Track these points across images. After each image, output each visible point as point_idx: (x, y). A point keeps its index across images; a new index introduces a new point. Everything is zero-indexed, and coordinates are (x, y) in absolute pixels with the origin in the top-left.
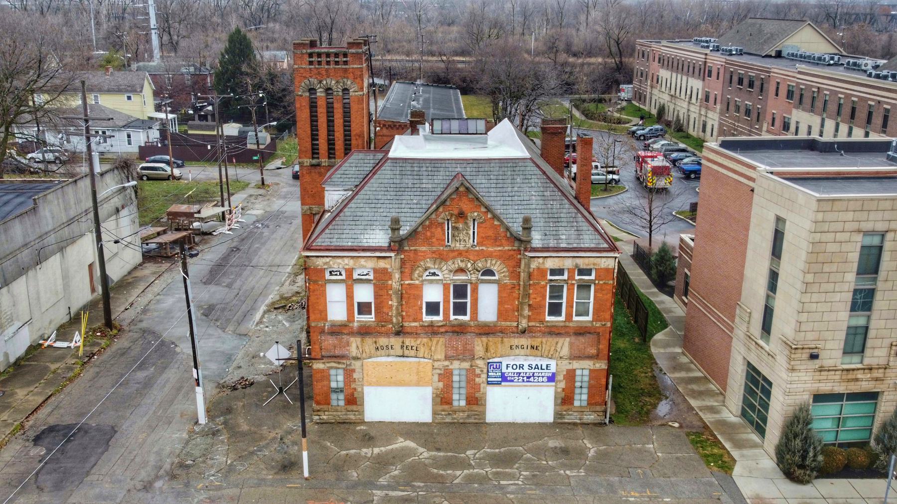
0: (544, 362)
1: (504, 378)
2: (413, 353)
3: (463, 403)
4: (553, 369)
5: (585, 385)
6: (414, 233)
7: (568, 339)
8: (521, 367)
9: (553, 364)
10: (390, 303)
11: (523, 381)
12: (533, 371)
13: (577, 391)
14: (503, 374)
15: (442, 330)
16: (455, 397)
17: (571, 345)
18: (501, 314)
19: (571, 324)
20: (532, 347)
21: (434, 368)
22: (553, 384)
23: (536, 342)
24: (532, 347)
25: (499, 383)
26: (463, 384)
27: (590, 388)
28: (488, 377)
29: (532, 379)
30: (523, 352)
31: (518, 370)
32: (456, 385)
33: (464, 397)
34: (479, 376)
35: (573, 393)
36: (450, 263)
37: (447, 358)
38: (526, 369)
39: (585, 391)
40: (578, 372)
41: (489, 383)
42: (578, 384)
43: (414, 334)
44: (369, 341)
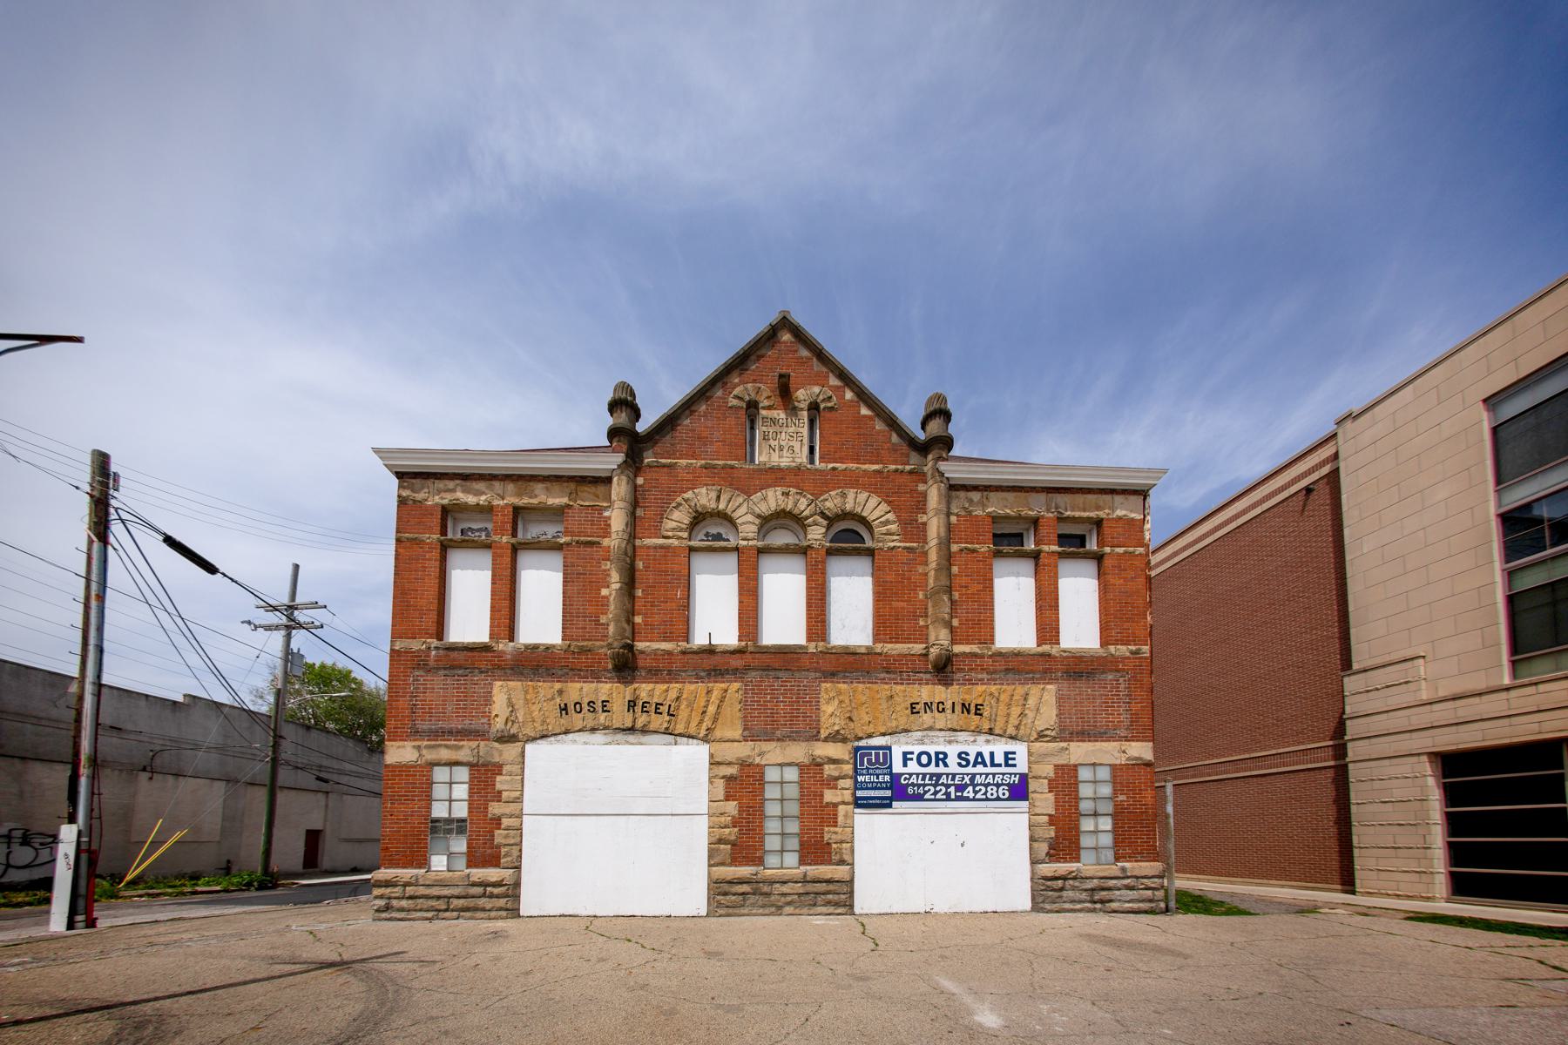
0: (999, 748)
1: (899, 791)
3: (792, 859)
4: (1022, 766)
5: (1108, 807)
8: (941, 758)
9: (1021, 750)
11: (948, 794)
12: (970, 770)
13: (1087, 825)
14: (896, 778)
15: (736, 662)
16: (772, 843)
17: (1060, 700)
18: (884, 625)
19: (1054, 651)
21: (714, 763)
22: (1025, 804)
23: (976, 693)
24: (965, 708)
25: (885, 804)
26: (793, 808)
27: (1117, 816)
28: (857, 786)
29: (969, 792)
30: (941, 720)
31: (932, 769)
32: (772, 809)
33: (794, 843)
34: (832, 782)
36: (757, 497)
37: (750, 735)
38: (953, 765)
39: (1106, 824)
40: (1084, 774)
41: (859, 803)
42: (1085, 806)
43: (665, 670)
44: (546, 688)
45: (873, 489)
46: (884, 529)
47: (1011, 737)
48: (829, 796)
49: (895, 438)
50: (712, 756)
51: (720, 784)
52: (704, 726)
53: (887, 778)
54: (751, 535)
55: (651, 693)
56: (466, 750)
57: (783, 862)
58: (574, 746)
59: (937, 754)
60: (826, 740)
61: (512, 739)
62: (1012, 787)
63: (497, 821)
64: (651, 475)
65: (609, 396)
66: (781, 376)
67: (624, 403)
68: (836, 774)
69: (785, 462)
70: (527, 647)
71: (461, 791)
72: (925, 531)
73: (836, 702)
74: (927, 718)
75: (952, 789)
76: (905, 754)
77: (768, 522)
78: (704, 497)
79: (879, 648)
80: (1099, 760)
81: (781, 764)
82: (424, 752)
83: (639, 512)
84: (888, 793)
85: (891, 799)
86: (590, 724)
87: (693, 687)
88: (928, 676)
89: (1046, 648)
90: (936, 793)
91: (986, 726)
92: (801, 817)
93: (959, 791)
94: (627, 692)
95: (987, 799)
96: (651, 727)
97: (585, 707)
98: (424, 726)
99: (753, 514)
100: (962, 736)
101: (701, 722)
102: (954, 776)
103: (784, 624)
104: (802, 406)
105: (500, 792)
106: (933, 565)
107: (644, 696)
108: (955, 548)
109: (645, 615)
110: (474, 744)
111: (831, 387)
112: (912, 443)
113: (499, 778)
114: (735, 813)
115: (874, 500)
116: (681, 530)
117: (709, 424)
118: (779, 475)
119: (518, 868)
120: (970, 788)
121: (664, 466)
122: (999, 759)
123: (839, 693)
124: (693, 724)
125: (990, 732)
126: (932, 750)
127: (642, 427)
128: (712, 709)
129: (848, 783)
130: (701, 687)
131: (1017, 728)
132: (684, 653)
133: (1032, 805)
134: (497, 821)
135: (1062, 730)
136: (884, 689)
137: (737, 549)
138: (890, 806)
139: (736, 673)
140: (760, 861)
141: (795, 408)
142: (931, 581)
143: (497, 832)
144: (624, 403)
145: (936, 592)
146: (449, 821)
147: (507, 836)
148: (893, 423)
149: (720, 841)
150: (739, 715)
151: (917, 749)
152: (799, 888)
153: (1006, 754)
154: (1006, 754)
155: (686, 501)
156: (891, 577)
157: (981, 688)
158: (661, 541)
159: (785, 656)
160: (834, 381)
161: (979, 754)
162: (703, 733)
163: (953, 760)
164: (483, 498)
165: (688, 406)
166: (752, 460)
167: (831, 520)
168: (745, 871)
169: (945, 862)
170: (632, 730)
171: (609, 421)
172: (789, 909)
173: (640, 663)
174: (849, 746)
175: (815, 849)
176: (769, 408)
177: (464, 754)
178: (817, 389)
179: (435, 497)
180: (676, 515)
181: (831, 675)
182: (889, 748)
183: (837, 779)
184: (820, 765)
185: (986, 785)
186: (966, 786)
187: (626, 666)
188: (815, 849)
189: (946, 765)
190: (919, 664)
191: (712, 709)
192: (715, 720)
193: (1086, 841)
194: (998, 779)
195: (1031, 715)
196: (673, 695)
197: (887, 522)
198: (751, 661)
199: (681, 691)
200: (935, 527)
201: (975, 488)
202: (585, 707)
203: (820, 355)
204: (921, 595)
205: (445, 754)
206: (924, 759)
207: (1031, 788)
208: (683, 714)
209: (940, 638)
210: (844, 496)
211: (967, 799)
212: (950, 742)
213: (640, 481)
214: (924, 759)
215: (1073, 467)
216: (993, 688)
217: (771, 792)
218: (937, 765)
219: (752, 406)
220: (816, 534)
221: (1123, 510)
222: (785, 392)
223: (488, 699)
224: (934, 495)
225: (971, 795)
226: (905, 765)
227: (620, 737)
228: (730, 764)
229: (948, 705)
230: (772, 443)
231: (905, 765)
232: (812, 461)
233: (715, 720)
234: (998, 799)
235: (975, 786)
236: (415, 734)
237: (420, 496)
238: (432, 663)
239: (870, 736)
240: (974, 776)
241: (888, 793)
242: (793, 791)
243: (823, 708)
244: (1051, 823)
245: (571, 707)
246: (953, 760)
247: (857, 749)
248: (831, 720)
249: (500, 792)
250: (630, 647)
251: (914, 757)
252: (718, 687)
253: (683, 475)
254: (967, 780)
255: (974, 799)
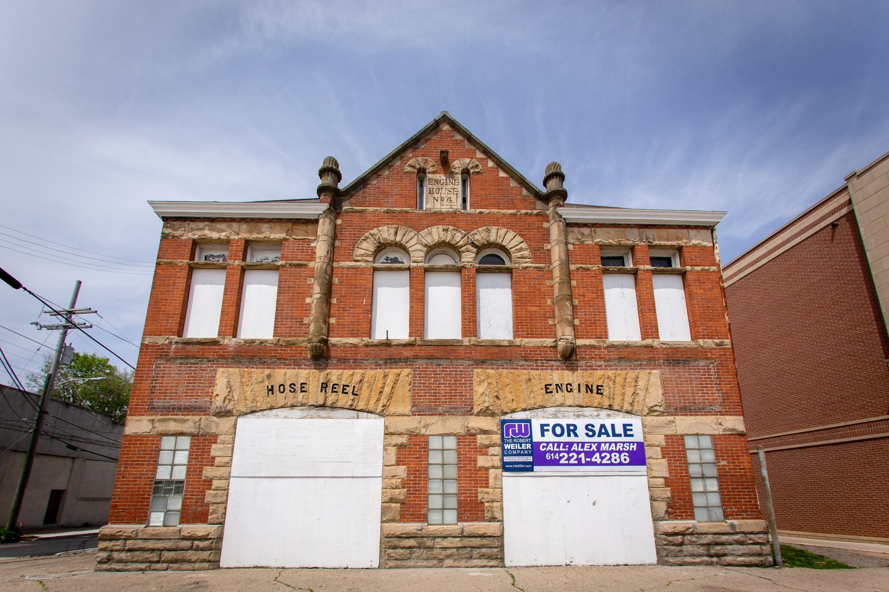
0: (619, 421)
1: (540, 457)
2: (345, 400)
3: (451, 516)
4: (638, 437)
6: (362, 183)
7: (656, 372)
8: (572, 429)
9: (636, 423)
10: (308, 300)
11: (579, 460)
12: (596, 439)
15: (407, 353)
16: (435, 502)
17: (664, 382)
20: (589, 388)
21: (388, 434)
22: (644, 468)
23: (596, 377)
25: (527, 468)
26: (452, 472)
29: (596, 458)
30: (570, 398)
31: (565, 438)
32: (435, 472)
33: (453, 502)
35: (689, 488)
37: (418, 411)
40: (690, 442)
42: (694, 470)
43: (351, 359)
44: (258, 373)
45: (510, 226)
46: (519, 254)
47: (628, 412)
48: (482, 461)
49: (524, 192)
50: (386, 428)
51: (393, 451)
52: (381, 404)
53: (529, 446)
54: (420, 259)
55: (340, 377)
56: (190, 424)
57: (443, 519)
58: (276, 420)
59: (568, 426)
60: (478, 414)
61: (227, 413)
62: (631, 453)
63: (209, 483)
64: (346, 217)
65: (320, 166)
66: (442, 152)
67: (331, 170)
68: (487, 442)
69: (445, 208)
70: (246, 341)
71: (182, 457)
72: (550, 255)
73: (486, 384)
74: (558, 397)
75: (582, 456)
76: (542, 426)
77: (432, 250)
78: (386, 233)
79: (518, 341)
80: (702, 431)
81: (442, 434)
82: (157, 424)
83: (337, 243)
84: (530, 459)
85: (533, 464)
86: (290, 401)
87: (373, 372)
88: (558, 363)
89: (649, 341)
90: (569, 459)
91: (606, 403)
92: (458, 479)
93: (588, 457)
94: (321, 376)
95: (612, 464)
96: (339, 404)
97: (288, 388)
98: (158, 403)
99: (421, 244)
100: (588, 411)
101: (378, 400)
102: (583, 444)
103: (444, 321)
104: (457, 171)
105: (213, 458)
106: (558, 280)
107: (334, 379)
108: (573, 267)
109: (338, 318)
110: (197, 418)
111: (477, 159)
112: (538, 195)
113: (214, 446)
114: (404, 475)
115: (511, 234)
116: (368, 255)
117: (391, 183)
118: (441, 217)
119: (222, 524)
120: (597, 455)
121: (357, 212)
122: (619, 430)
123: (488, 377)
124: (372, 402)
125: (610, 408)
126: (564, 422)
127: (342, 186)
128: (387, 390)
129: (497, 450)
130: (379, 372)
131: (632, 404)
132: (366, 346)
133: (650, 469)
134: (209, 483)
135: (668, 406)
136: (524, 374)
137: (409, 269)
138: (531, 470)
139: (407, 361)
140: (424, 518)
141: (452, 172)
142: (556, 292)
143: (208, 492)
144: (331, 170)
145: (560, 300)
146: (170, 482)
147: (215, 496)
148: (522, 182)
149: (392, 500)
150: (409, 394)
151: (552, 422)
152: (457, 542)
153: (625, 426)
154: (625, 426)
155: (372, 235)
156: (526, 289)
157: (600, 373)
158: (353, 264)
159: (445, 348)
160: (479, 155)
161: (603, 426)
162: (380, 408)
163: (581, 431)
164: (224, 234)
165: (376, 172)
166: (421, 207)
167: (479, 248)
168: (411, 527)
169: (580, 515)
170: (323, 406)
171: (319, 182)
172: (448, 562)
173: (333, 354)
174: (497, 419)
175: (471, 508)
176: (434, 173)
177: (188, 427)
178: (467, 160)
179: (189, 234)
180: (365, 245)
181: (481, 363)
182: (529, 421)
183: (487, 447)
184: (473, 435)
185: (611, 452)
186: (593, 453)
187: (321, 356)
188: (471, 508)
189: (576, 435)
190: (550, 354)
191: (387, 390)
192: (390, 398)
193: (698, 501)
194: (620, 447)
195: (642, 394)
196: (357, 378)
197: (521, 249)
198: (419, 352)
199: (363, 376)
200: (557, 253)
201: (585, 225)
202: (288, 388)
203: (470, 138)
204: (549, 302)
205: (173, 426)
206: (558, 430)
207: (647, 455)
208: (364, 394)
209: (565, 334)
210: (488, 231)
211: (595, 464)
212: (578, 416)
213: (339, 222)
214: (558, 430)
215: (656, 211)
216: (610, 373)
217: (434, 458)
218: (569, 435)
219: (422, 172)
220: (469, 258)
221: (697, 239)
222: (445, 162)
223: (212, 382)
224: (555, 230)
225: (598, 461)
226: (543, 435)
227: (313, 412)
228: (400, 434)
229: (575, 386)
230: (436, 196)
231: (543, 435)
232: (465, 208)
233: (390, 398)
234: (621, 464)
235: (601, 453)
236: (152, 409)
237: (177, 233)
238: (171, 354)
239: (513, 411)
240: (599, 444)
241: (530, 459)
242: (452, 457)
243: (476, 388)
244: (667, 484)
245: (276, 388)
246: (581, 431)
247: (503, 422)
248: (482, 399)
249: (213, 458)
250: (325, 342)
251: (550, 428)
252: (392, 372)
253: (370, 217)
254: (594, 447)
255: (601, 464)
